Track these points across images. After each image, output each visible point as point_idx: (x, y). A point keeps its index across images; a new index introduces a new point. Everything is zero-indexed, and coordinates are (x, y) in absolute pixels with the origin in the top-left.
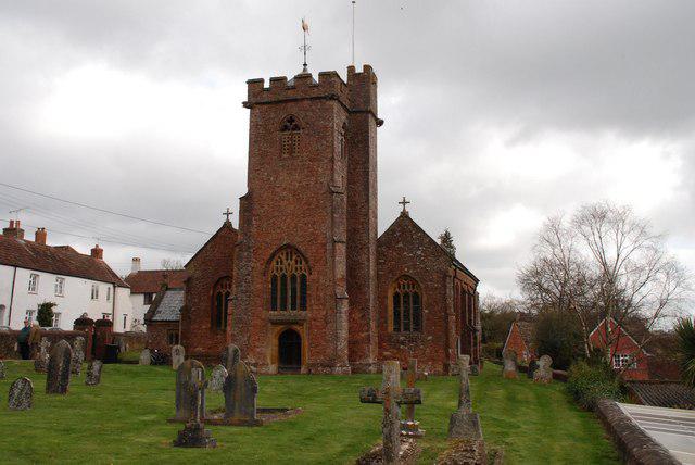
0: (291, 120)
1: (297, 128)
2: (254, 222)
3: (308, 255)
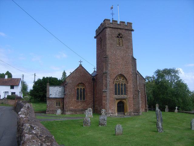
0: (119, 35)
1: (121, 37)
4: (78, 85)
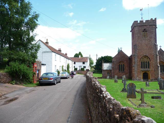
0: (145, 30)
1: (146, 31)
3: (150, 58)
4: (120, 62)
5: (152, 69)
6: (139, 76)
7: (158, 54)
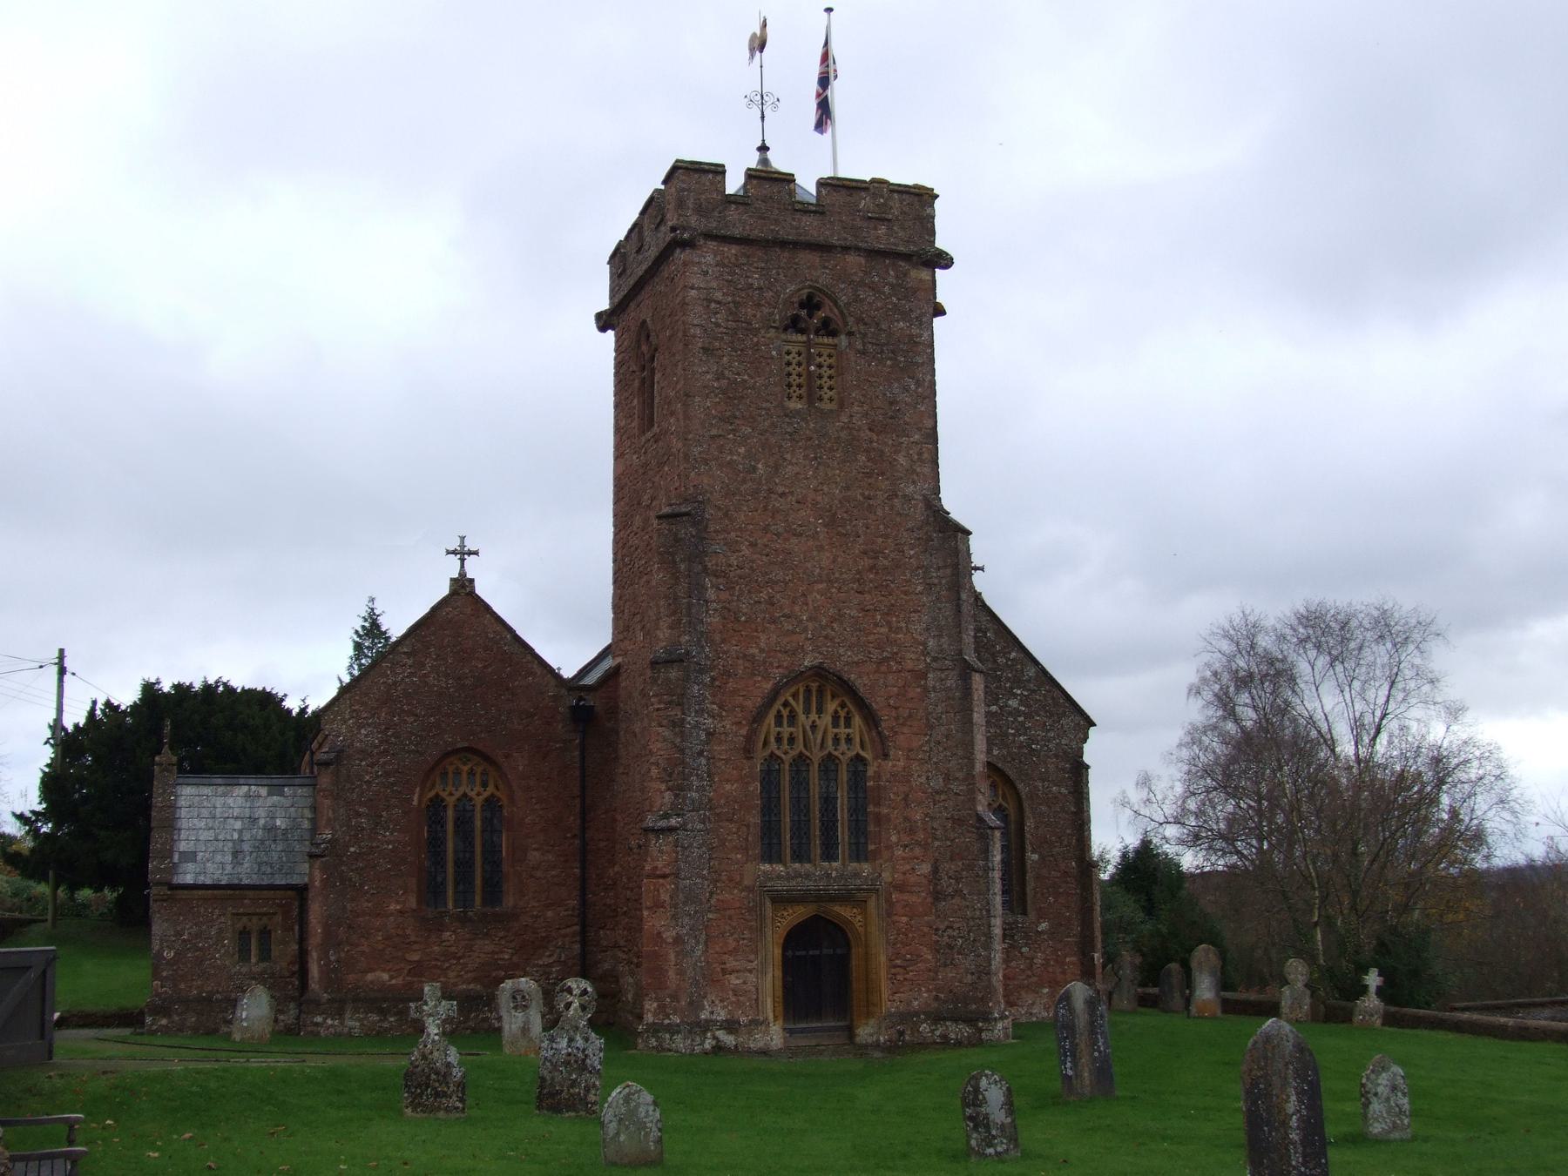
0: (810, 304)
1: (827, 328)
2: (711, 594)
3: (877, 703)
5: (900, 864)
6: (734, 980)
7: (970, 657)
